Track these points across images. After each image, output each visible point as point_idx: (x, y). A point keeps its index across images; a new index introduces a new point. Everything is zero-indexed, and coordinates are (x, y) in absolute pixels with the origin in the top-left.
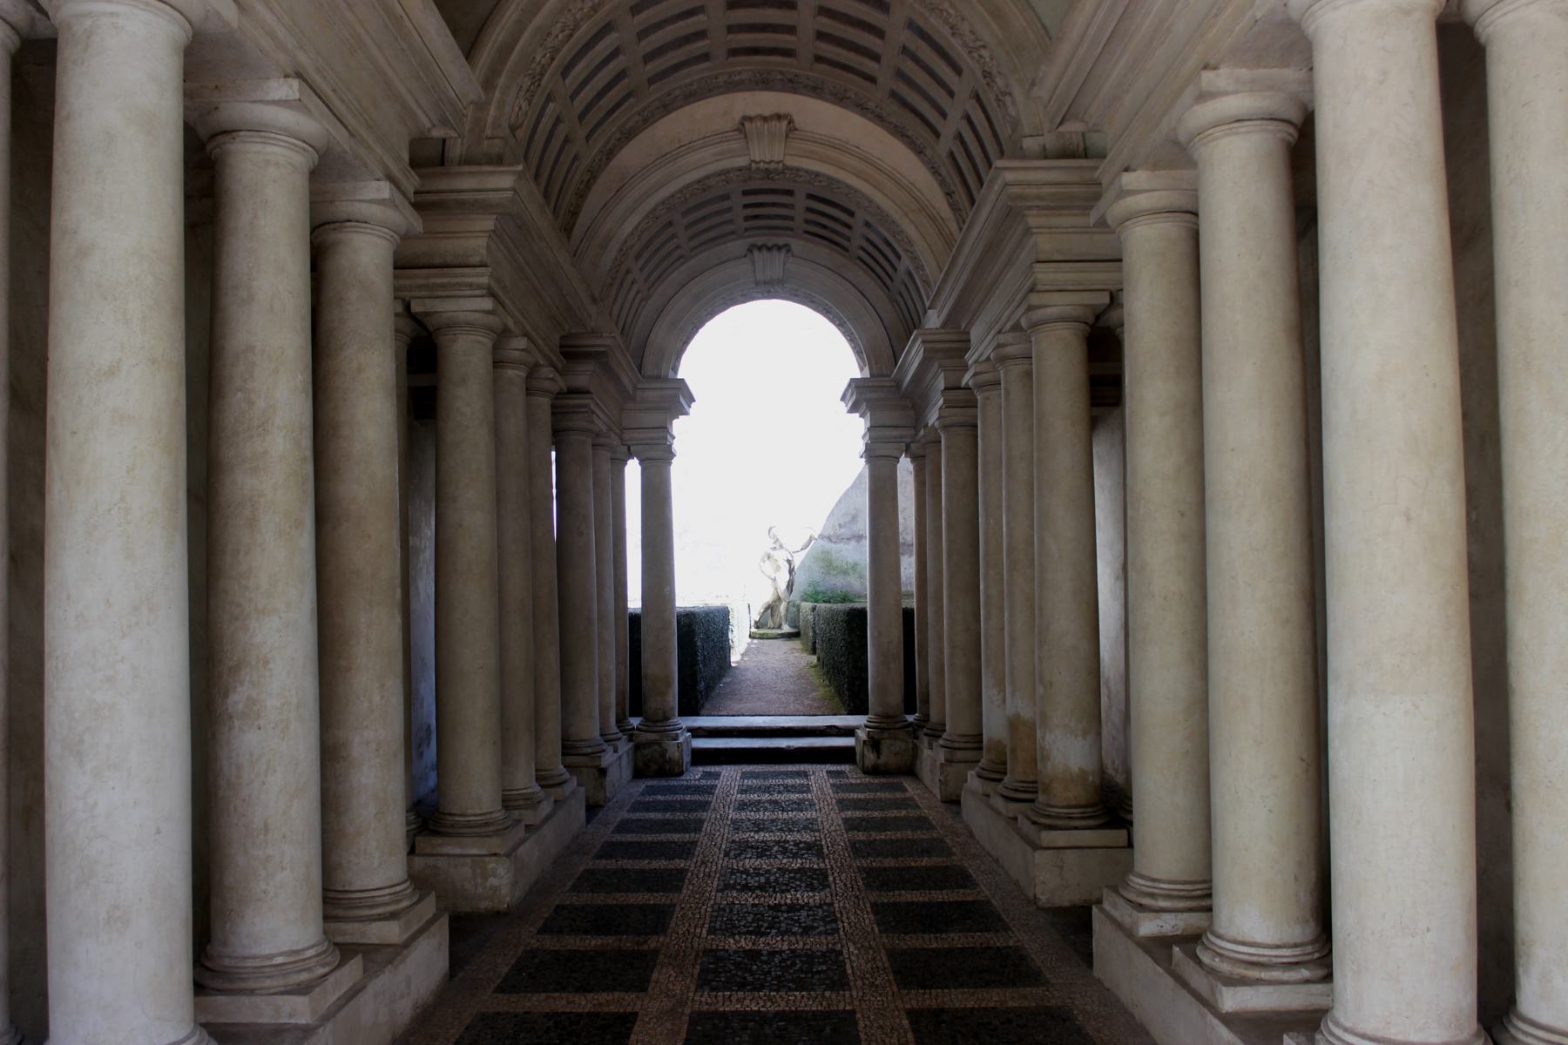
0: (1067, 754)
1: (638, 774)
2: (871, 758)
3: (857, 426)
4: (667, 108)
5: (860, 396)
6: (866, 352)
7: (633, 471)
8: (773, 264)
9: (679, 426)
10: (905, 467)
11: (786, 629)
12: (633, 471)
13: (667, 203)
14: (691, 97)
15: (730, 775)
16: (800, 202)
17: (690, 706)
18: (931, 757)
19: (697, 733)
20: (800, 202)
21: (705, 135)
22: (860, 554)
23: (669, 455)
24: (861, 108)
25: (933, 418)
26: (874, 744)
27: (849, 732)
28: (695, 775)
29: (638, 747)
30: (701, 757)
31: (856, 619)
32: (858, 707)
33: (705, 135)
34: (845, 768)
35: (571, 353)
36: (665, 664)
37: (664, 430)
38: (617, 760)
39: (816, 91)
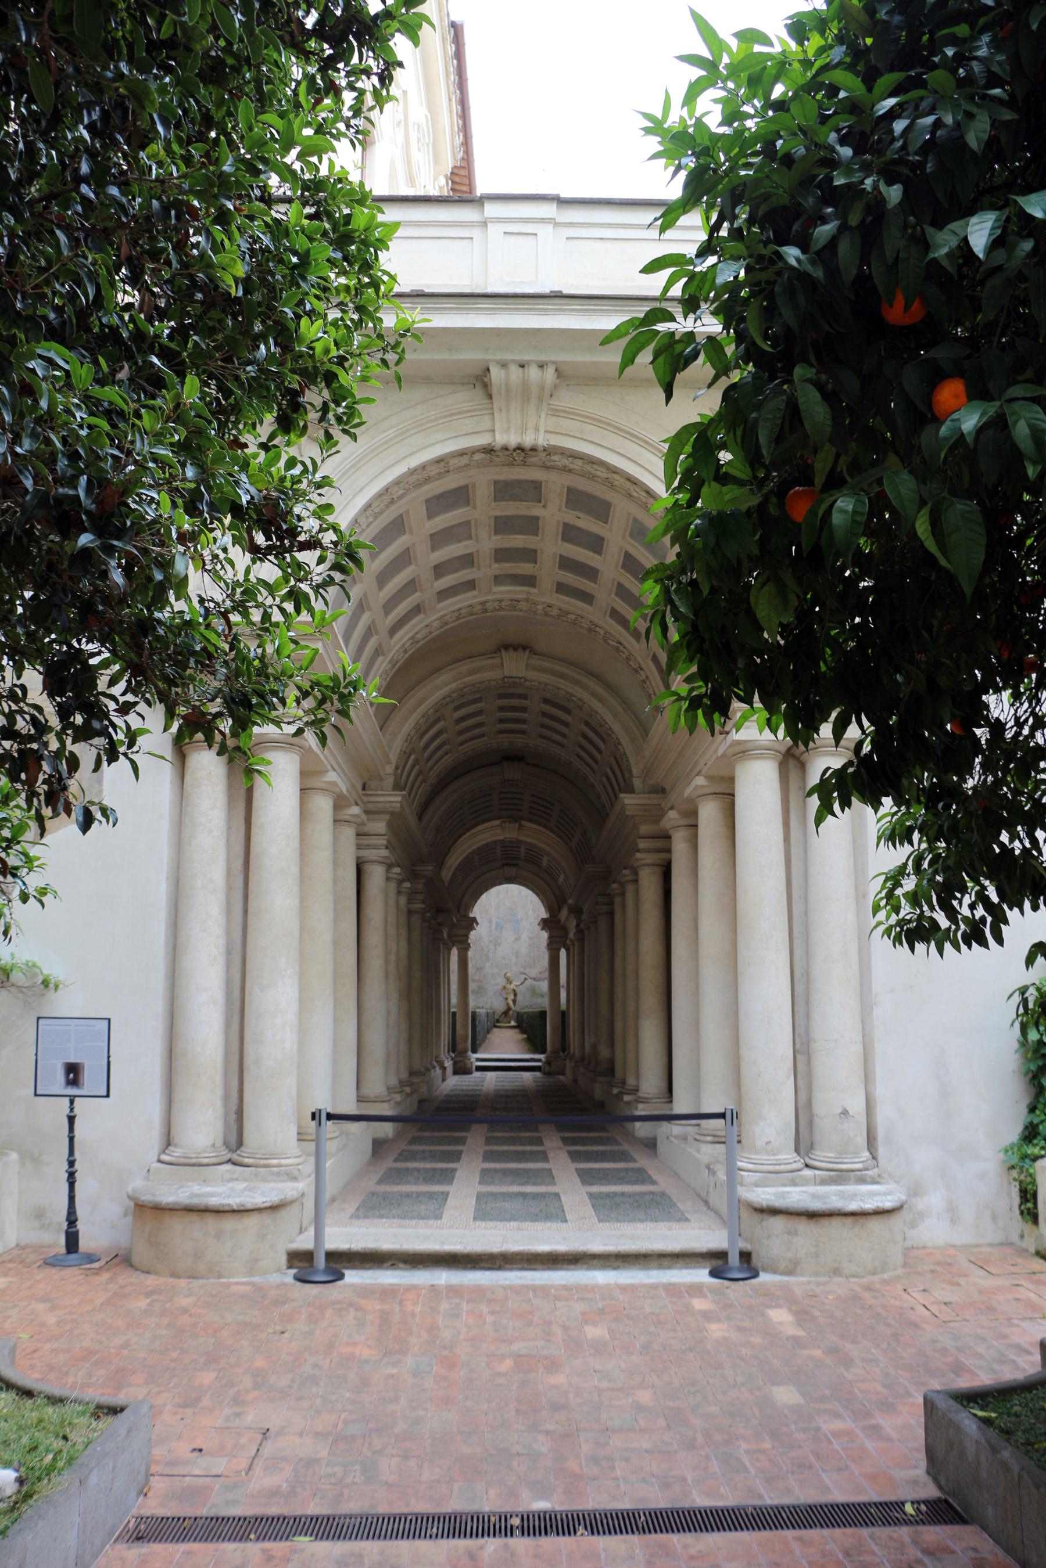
0: (604, 1052)
1: (456, 1072)
2: (547, 1068)
3: (545, 935)
4: (476, 825)
5: (545, 924)
6: (549, 907)
7: (455, 952)
8: (512, 871)
9: (473, 935)
10: (563, 953)
11: (513, 1023)
12: (455, 952)
13: (473, 853)
14: (484, 821)
15: (490, 1075)
16: (523, 851)
17: (474, 1051)
18: (569, 1065)
19: (478, 1060)
20: (523, 851)
21: (488, 833)
22: (544, 986)
23: (467, 947)
24: (546, 827)
25: (571, 935)
26: (548, 1062)
27: (539, 1060)
28: (477, 1074)
29: (455, 1064)
30: (480, 1069)
31: (543, 1014)
32: (543, 1052)
33: (488, 833)
34: (538, 1074)
35: (439, 910)
36: (464, 1030)
37: (467, 936)
38: (448, 1064)
39: (530, 821)
